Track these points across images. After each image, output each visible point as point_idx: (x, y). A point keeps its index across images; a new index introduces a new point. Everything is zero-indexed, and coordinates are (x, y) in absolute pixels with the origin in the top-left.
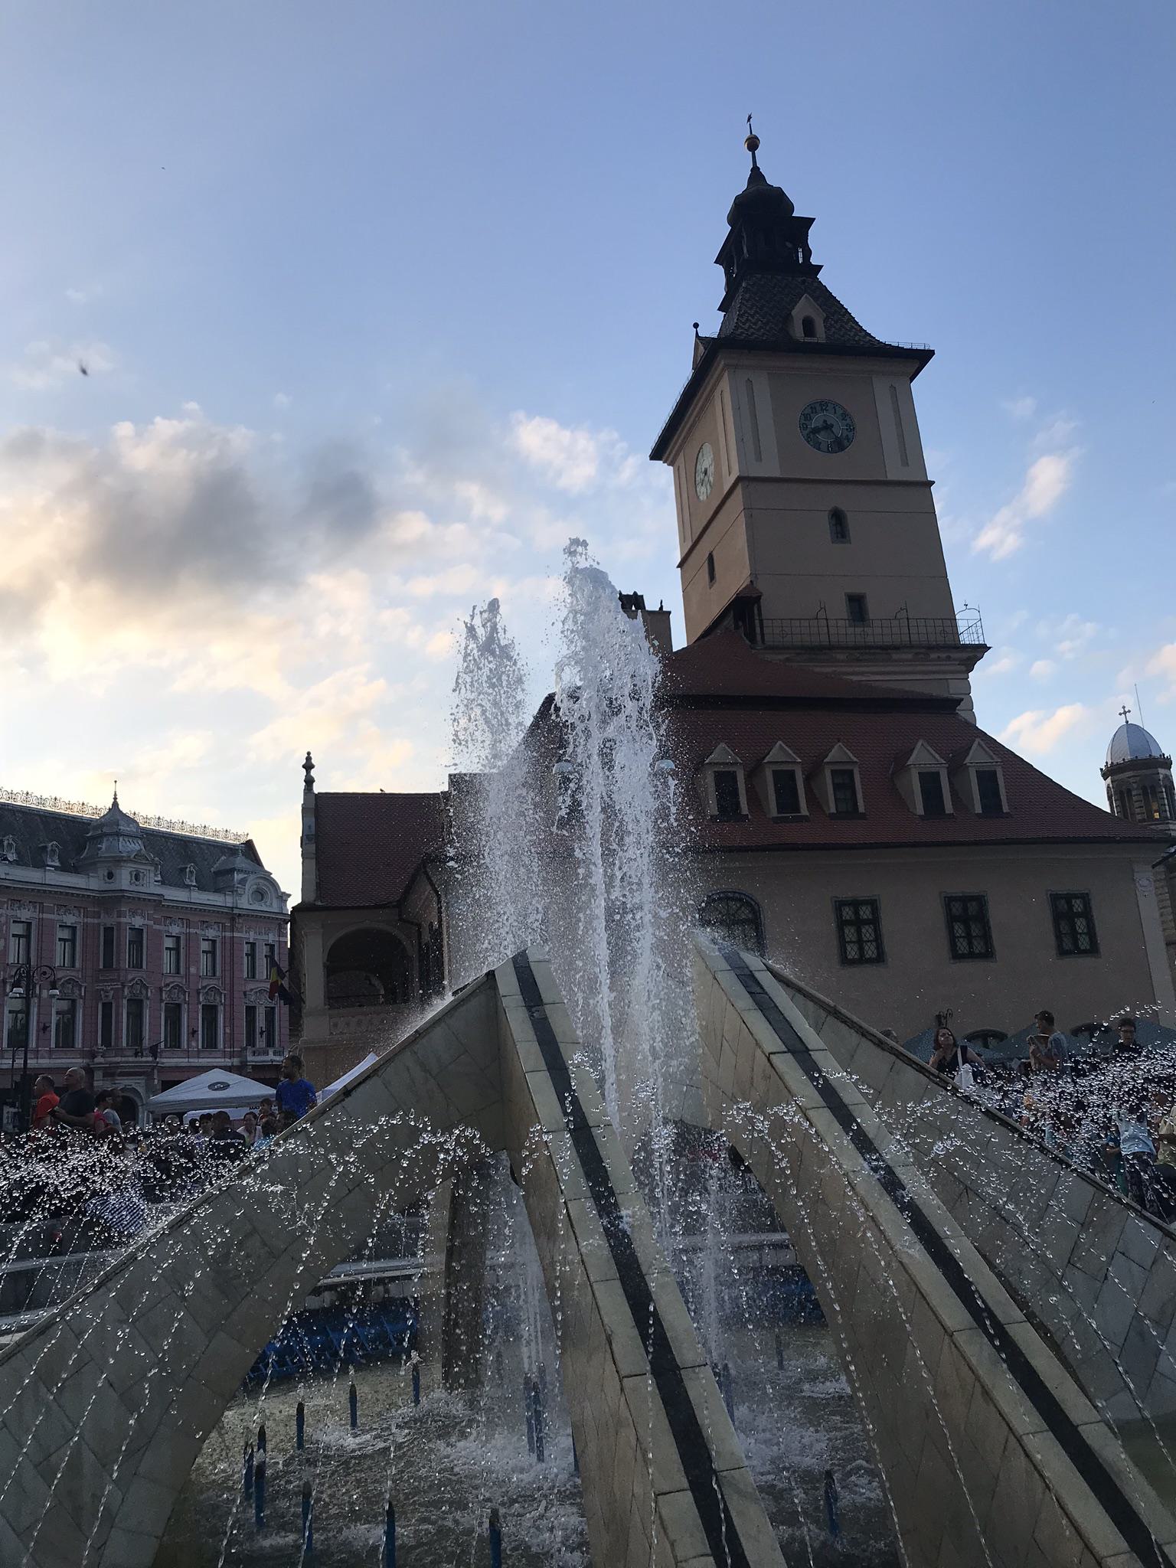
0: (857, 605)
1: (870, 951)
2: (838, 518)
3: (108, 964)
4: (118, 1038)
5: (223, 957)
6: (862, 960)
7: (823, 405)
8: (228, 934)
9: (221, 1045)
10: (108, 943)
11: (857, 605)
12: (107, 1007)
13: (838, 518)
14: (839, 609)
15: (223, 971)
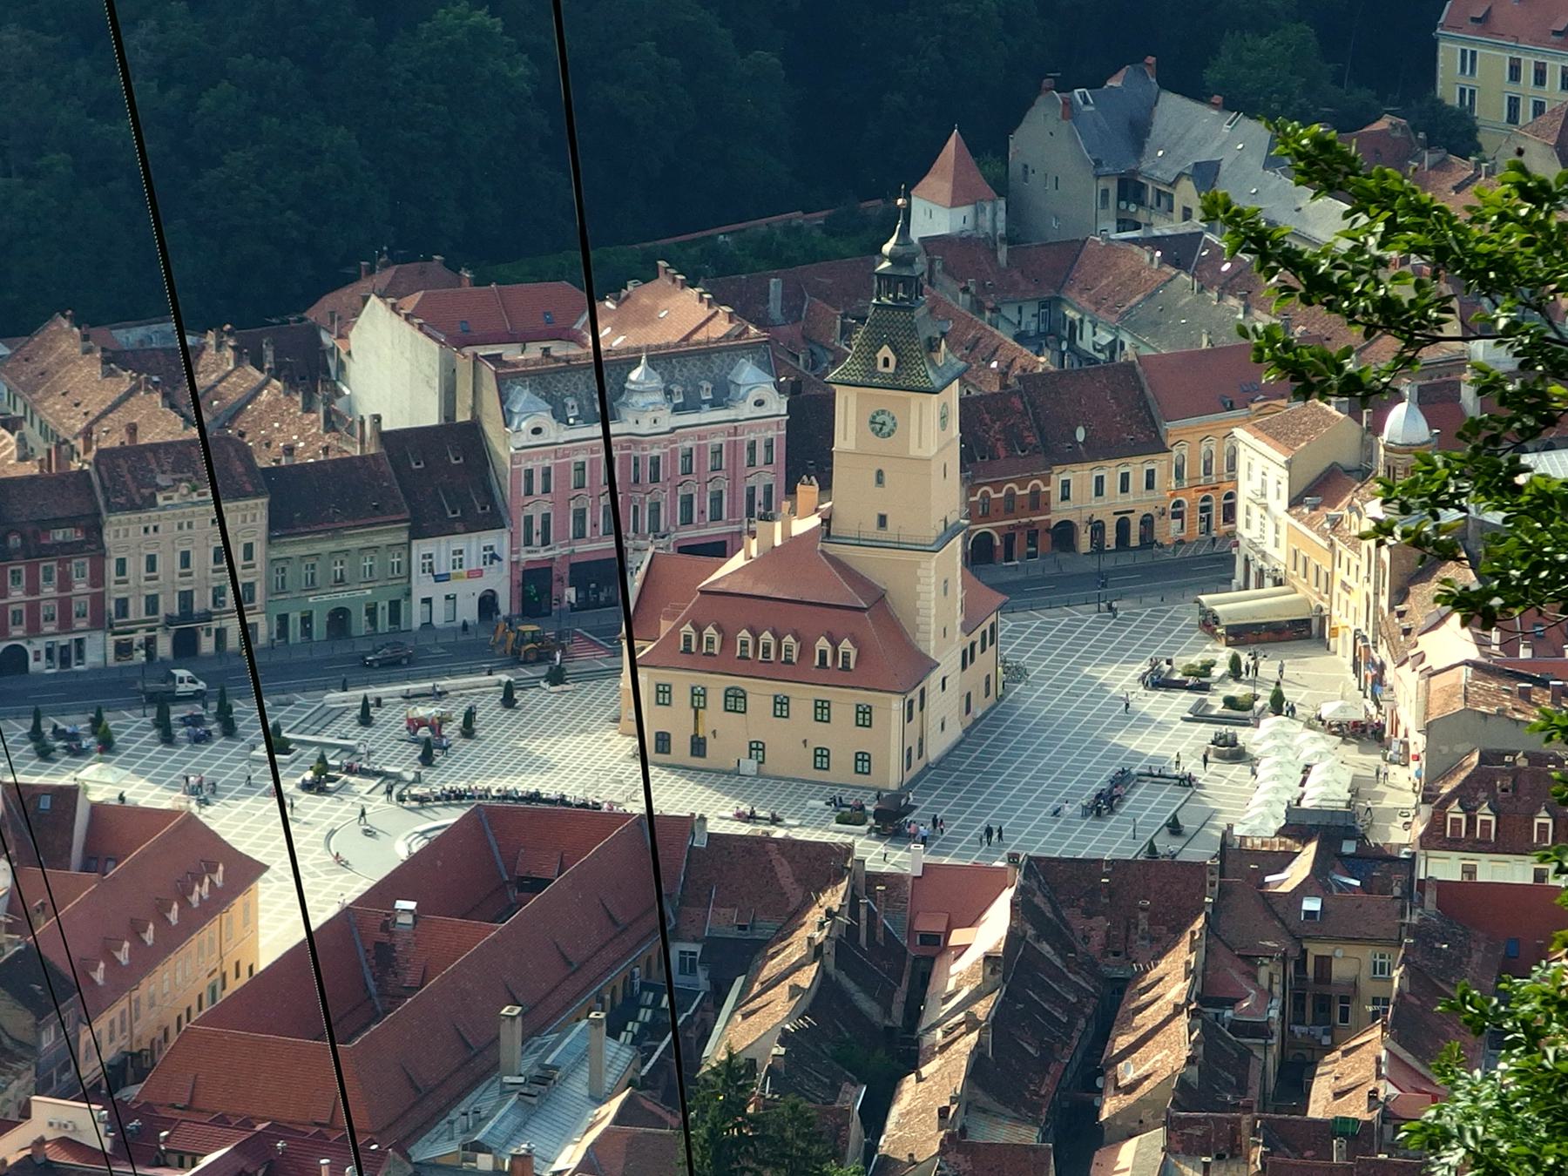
0: (882, 521)
1: (785, 714)
2: (880, 473)
3: (636, 481)
4: (643, 529)
5: (728, 455)
6: (781, 716)
7: (883, 412)
8: (733, 438)
9: (725, 516)
10: (636, 465)
11: (882, 521)
12: (636, 508)
13: (880, 473)
14: (875, 520)
15: (728, 464)
